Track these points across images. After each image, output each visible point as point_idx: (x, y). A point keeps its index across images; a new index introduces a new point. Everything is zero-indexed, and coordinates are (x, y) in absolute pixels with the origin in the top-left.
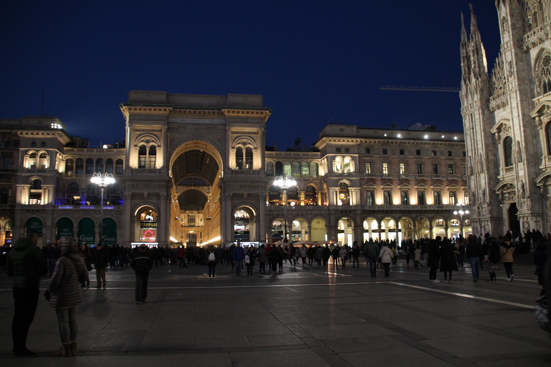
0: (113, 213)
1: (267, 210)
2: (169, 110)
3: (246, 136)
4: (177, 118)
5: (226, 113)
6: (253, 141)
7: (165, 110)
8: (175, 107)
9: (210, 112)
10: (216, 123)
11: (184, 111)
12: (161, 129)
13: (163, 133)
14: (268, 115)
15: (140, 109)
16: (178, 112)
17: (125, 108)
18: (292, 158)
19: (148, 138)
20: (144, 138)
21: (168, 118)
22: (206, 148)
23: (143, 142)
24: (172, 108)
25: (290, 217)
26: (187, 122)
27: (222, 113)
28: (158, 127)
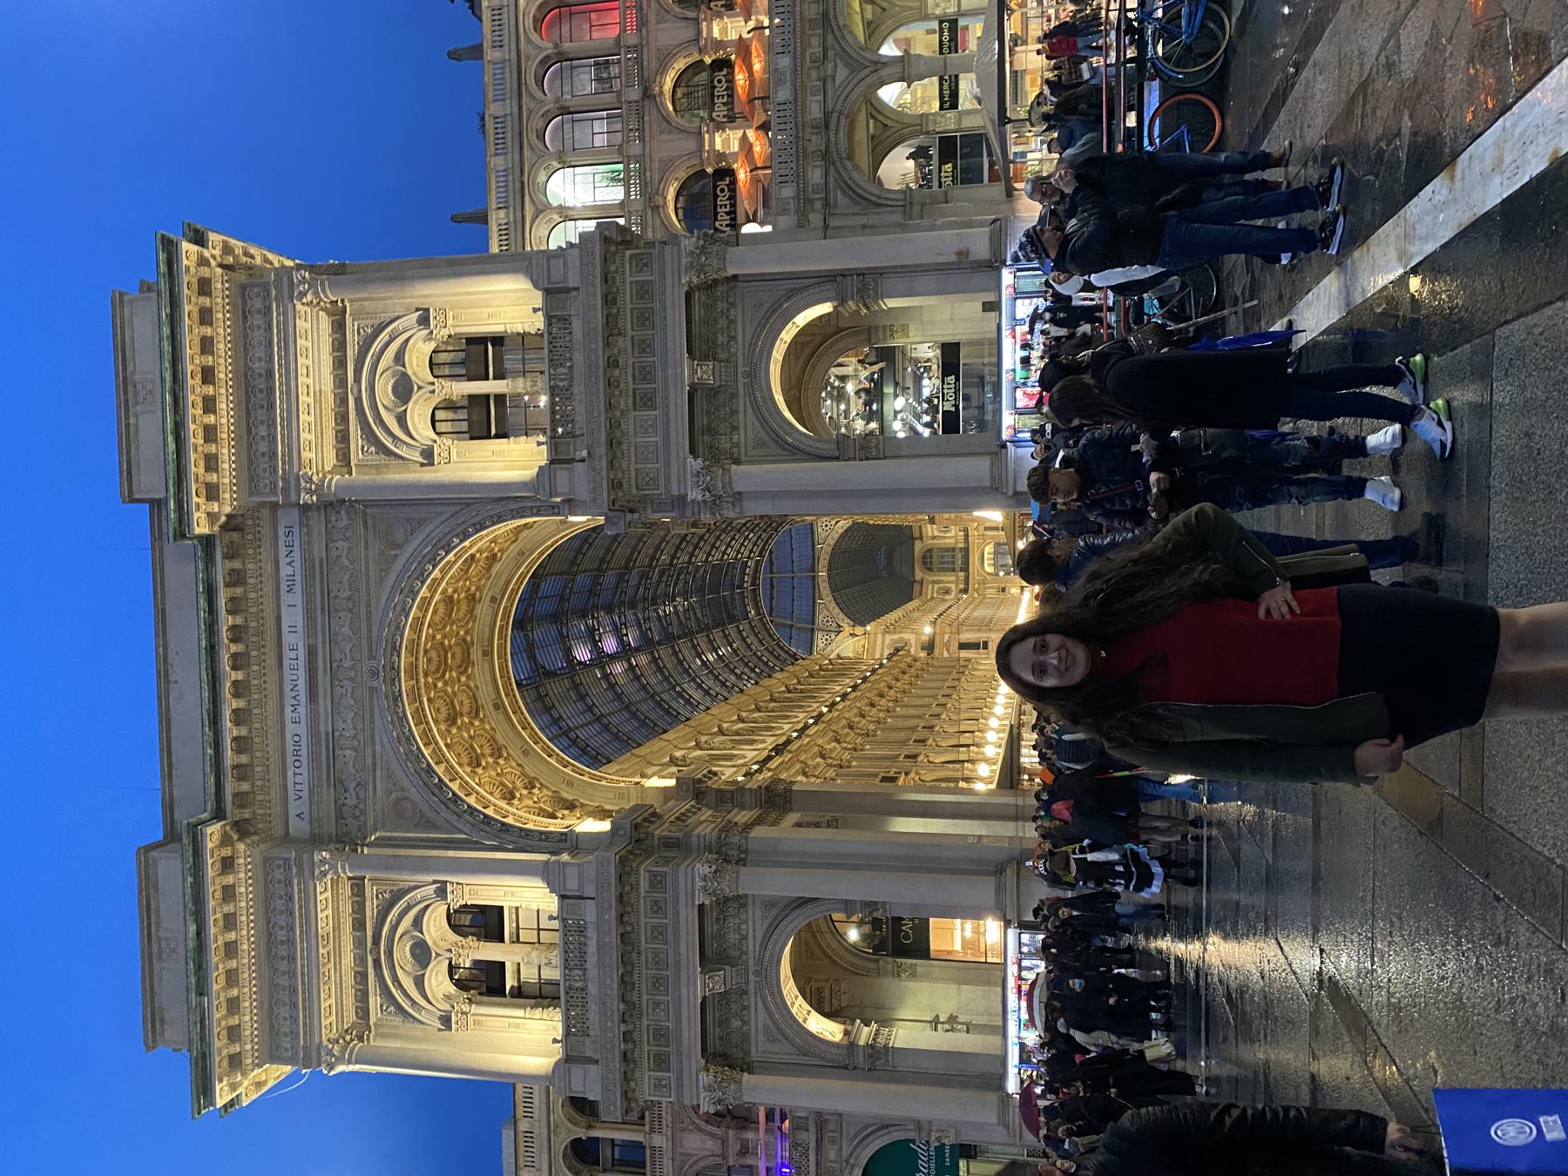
0: (832, 1155)
1: (800, 226)
3: (357, 380)
6: (384, 337)
7: (227, 865)
9: (232, 600)
10: (297, 564)
12: (350, 878)
14: (227, 249)
15: (233, 1006)
16: (245, 787)
17: (233, 1087)
18: (520, 108)
19: (403, 953)
20: (399, 972)
21: (287, 839)
22: (493, 600)
25: (842, 74)
26: (302, 729)
27: (224, 527)
28: (336, 896)
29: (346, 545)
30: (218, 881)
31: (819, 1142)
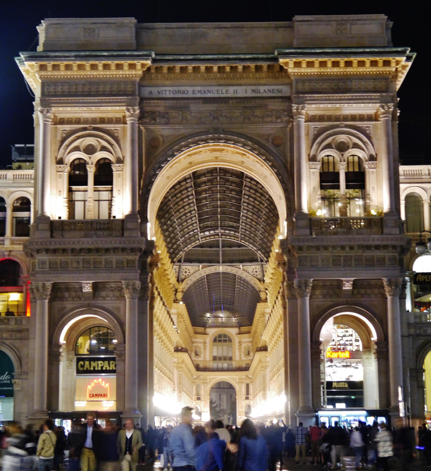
0: (5, 335)
2: (143, 65)
3: (346, 126)
4: (165, 86)
5: (291, 69)
6: (365, 139)
7: (132, 67)
8: (158, 57)
9: (249, 67)
10: (264, 95)
11: (181, 68)
12: (124, 117)
13: (128, 126)
14: (404, 67)
15: (68, 67)
16: (165, 71)
22: (243, 162)
23: (80, 151)
24: (149, 62)
26: (190, 95)
27: (281, 68)
28: (116, 112)
29: (274, 119)
30: (126, 64)
31: (12, 331)
